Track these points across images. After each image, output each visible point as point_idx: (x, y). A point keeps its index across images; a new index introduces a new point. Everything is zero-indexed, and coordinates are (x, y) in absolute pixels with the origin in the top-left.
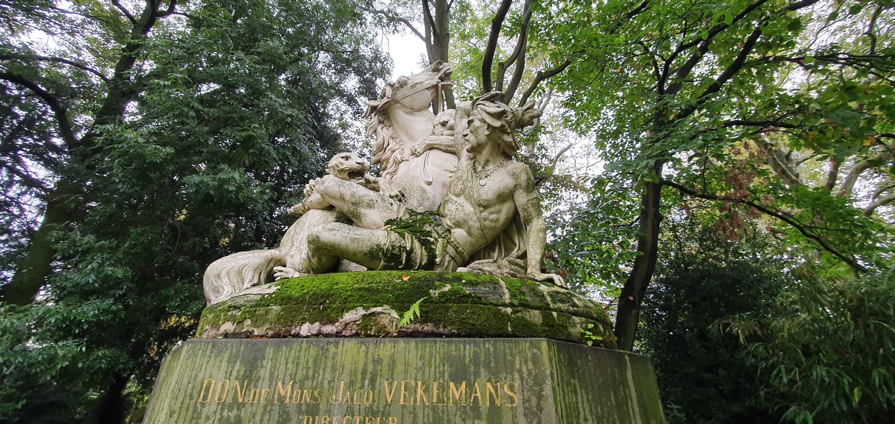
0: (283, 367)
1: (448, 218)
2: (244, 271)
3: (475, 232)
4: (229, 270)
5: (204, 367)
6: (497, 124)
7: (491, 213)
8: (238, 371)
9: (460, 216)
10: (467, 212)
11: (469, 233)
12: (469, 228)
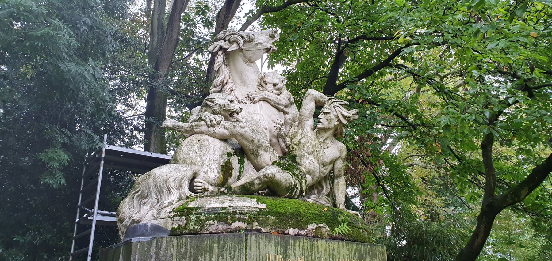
0: (298, 250)
1: (303, 167)
2: (183, 180)
3: (316, 178)
4: (176, 179)
5: (264, 247)
6: (345, 122)
7: (324, 170)
8: (280, 251)
9: (311, 168)
10: (316, 167)
11: (313, 179)
12: (314, 176)
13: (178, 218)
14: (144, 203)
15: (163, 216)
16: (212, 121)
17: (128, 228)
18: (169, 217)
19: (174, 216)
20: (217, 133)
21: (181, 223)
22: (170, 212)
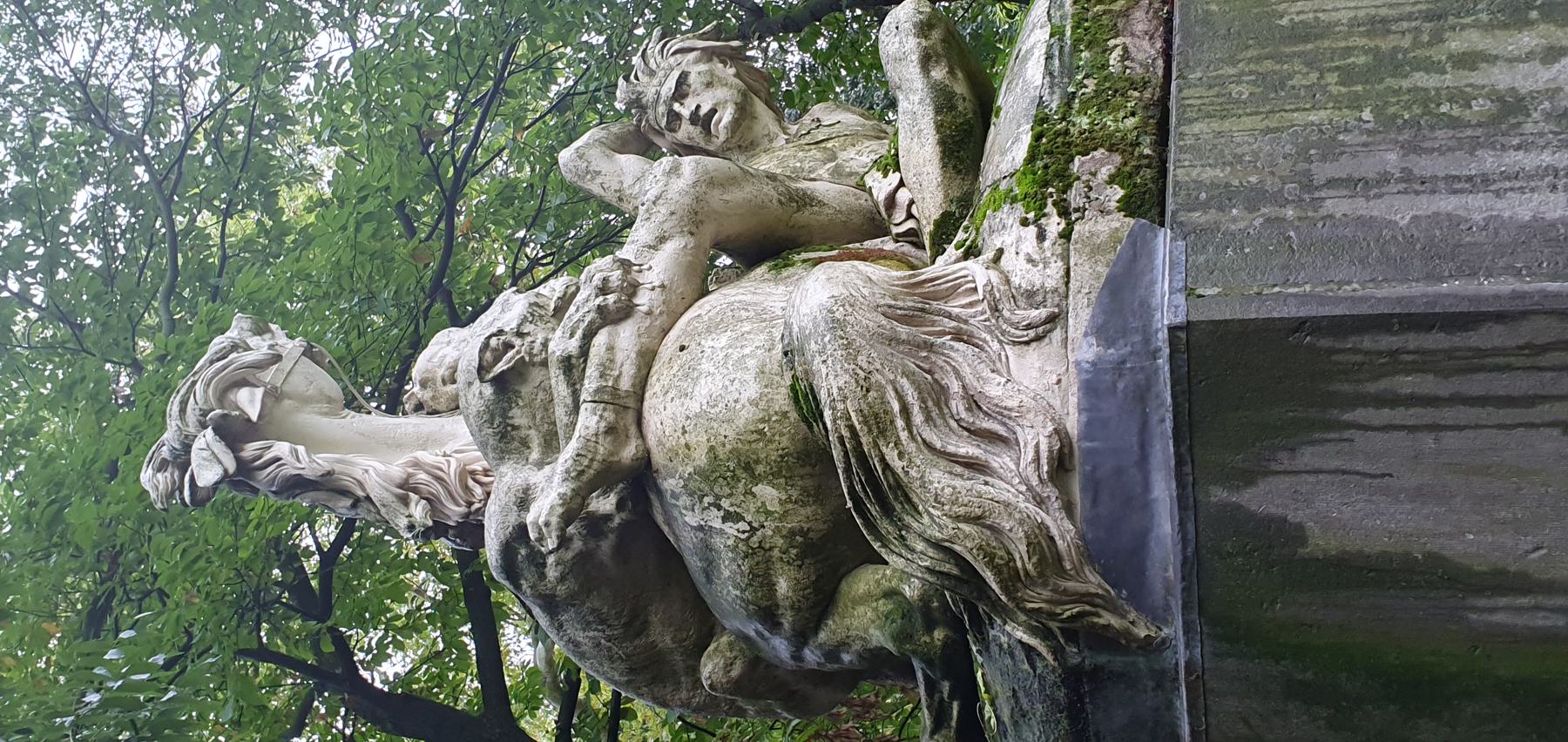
13: (1075, 197)
14: (973, 403)
15: (1052, 275)
16: (605, 280)
17: (1091, 552)
18: (1066, 235)
19: (1064, 212)
20: (672, 282)
21: (1104, 173)
22: (1041, 236)
